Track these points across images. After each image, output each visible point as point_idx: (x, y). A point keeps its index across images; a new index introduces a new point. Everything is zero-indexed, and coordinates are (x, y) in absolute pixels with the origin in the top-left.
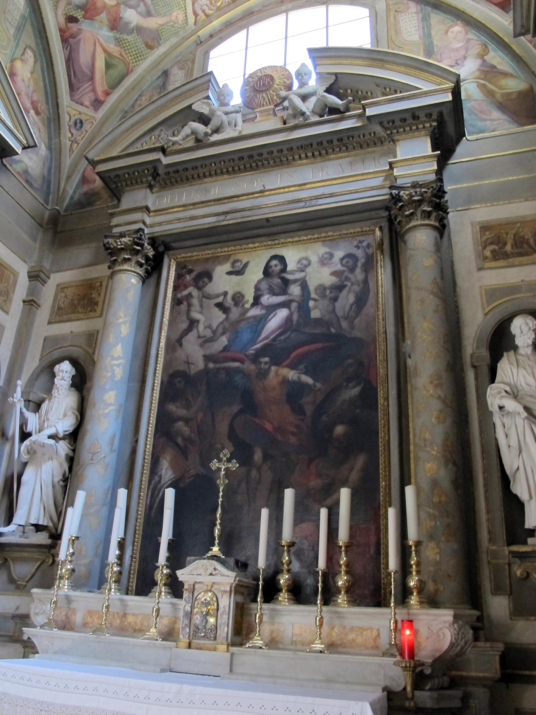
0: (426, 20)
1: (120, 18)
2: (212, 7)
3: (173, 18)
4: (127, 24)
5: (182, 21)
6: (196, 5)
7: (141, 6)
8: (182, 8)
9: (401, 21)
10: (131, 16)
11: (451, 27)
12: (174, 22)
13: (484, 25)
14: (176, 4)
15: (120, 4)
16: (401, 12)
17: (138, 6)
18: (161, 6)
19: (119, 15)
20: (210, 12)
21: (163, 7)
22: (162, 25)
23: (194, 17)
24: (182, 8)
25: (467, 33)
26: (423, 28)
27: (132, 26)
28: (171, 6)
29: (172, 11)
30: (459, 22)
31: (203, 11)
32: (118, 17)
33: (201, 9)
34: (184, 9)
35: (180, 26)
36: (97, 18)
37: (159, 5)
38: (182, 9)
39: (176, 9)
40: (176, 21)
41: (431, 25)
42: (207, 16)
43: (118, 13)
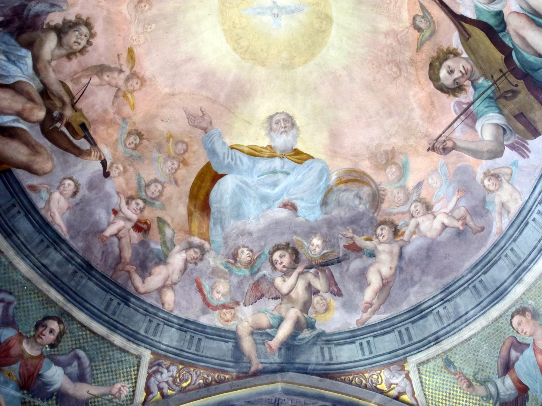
1: (39, 376)
2: (174, 387)
3: (115, 390)
4: (46, 385)
5: (126, 396)
6: (153, 379)
7: (73, 365)
8: (132, 379)
10: (55, 376)
12: (114, 395)
14: (123, 373)
15: (44, 357)
17: (70, 364)
18: (102, 371)
19: (39, 370)
20: (170, 392)
21: (104, 373)
22: (96, 397)
23: (145, 394)
24: (132, 379)
27: (52, 389)
28: (116, 375)
29: (115, 381)
31: (160, 389)
32: (36, 374)
33: (158, 385)
34: (134, 381)
35: (121, 403)
36: (6, 368)
37: (100, 369)
38: (130, 382)
39: (123, 379)
40: (117, 395)
42: (163, 396)
43: (37, 367)
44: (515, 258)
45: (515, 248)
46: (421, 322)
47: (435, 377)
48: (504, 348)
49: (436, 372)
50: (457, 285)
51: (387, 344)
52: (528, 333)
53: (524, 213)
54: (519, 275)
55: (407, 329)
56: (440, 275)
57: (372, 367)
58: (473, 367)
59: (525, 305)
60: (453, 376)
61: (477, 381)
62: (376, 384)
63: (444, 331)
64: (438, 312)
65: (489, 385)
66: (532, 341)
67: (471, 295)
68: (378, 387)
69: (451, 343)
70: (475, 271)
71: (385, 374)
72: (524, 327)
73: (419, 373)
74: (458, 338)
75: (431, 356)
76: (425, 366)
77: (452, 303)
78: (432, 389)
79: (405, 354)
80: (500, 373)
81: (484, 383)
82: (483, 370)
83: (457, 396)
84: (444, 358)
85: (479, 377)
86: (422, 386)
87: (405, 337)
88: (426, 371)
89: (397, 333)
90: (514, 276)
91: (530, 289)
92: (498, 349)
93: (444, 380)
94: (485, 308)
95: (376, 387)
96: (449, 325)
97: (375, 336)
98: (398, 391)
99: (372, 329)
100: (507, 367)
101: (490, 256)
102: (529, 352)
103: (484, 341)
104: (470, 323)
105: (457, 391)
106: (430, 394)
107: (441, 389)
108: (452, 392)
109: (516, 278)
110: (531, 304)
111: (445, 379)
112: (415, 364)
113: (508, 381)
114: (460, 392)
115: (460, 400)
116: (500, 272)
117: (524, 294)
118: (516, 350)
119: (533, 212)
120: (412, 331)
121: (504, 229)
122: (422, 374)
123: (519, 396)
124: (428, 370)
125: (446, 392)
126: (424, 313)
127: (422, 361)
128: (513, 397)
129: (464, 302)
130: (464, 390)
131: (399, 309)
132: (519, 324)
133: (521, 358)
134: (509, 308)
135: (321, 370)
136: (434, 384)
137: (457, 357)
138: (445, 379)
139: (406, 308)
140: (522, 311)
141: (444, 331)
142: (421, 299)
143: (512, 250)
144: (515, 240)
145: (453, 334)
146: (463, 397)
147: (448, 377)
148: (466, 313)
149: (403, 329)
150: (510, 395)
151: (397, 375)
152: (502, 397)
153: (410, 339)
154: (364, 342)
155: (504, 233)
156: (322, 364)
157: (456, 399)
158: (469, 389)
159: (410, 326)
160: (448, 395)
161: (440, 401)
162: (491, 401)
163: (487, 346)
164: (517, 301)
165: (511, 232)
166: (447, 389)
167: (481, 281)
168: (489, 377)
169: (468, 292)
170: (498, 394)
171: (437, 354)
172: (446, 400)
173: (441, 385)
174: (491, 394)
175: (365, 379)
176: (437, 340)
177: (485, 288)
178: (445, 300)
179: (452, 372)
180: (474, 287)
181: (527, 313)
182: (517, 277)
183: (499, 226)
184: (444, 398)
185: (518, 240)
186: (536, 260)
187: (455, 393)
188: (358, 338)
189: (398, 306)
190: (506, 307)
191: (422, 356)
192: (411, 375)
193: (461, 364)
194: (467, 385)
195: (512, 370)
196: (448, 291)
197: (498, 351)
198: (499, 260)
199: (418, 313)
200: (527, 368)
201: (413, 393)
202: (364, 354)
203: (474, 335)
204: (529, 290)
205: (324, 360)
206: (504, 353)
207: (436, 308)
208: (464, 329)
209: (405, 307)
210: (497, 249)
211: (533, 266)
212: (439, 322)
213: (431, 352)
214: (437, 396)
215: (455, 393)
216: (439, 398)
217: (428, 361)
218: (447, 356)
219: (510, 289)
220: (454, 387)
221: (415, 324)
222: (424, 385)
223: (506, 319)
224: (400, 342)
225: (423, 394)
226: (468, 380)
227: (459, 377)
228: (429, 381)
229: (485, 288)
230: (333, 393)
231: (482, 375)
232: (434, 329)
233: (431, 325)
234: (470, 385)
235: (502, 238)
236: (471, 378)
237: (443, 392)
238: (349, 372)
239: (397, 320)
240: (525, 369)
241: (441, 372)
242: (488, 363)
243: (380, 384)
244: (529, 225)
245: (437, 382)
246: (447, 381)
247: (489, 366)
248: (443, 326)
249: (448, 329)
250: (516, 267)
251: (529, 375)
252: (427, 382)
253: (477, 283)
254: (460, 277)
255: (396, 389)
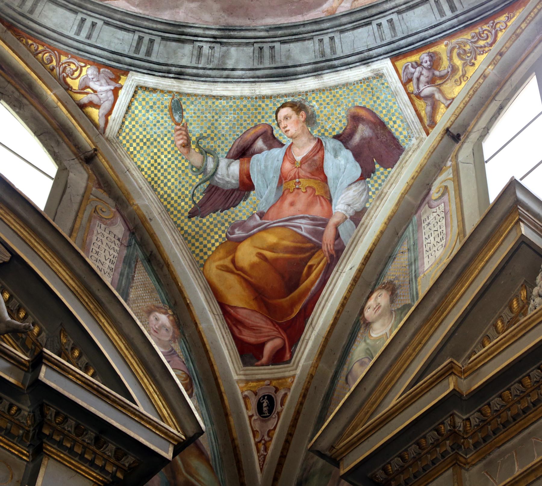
0: (130, 266)
9: (95, 232)
11: (158, 309)
13: (207, 351)
16: (101, 219)
25: (174, 339)
26: (122, 274)
30: (170, 312)
41: (133, 280)
44: (329, 50)
45: (337, 40)
46: (174, 44)
47: (151, 113)
48: (252, 132)
49: (155, 107)
50: (243, 34)
51: (116, 41)
52: (290, 133)
53: (374, 11)
54: (322, 69)
55: (152, 41)
56: (230, 10)
57: (78, 54)
58: (205, 129)
59: (306, 104)
60: (173, 124)
61: (198, 146)
62: (68, 76)
63: (195, 71)
64: (201, 48)
65: (210, 159)
66: (289, 144)
67: (251, 54)
68: (69, 80)
69: (194, 88)
70: (272, 33)
71: (89, 71)
72: (290, 125)
73: (133, 96)
74: (206, 89)
75: (160, 87)
76: (147, 93)
77: (224, 48)
78: (137, 122)
79: (130, 65)
80: (231, 155)
81: (205, 153)
82: (212, 139)
83: (162, 147)
84: (175, 99)
85: (203, 143)
86: (127, 112)
87: (143, 49)
88: (144, 99)
89: (136, 37)
90: (314, 66)
91: (324, 90)
92: (245, 128)
93: (158, 122)
94: (258, 77)
95: (64, 78)
96: (204, 69)
97: (106, 23)
98: (91, 99)
99: (109, 13)
100: (243, 152)
101: (302, 29)
102: (278, 153)
103: (234, 110)
104: (231, 82)
105: (166, 142)
106: (130, 126)
107: (148, 129)
108: (159, 139)
109: (315, 70)
110: (313, 107)
111: (162, 122)
112: (135, 84)
113: (235, 167)
114: (169, 146)
115: (162, 153)
116: (302, 53)
117: (313, 91)
118: (265, 142)
119: (384, 16)
120: (156, 47)
121: (337, 12)
122: (135, 99)
123: (238, 190)
124: (147, 99)
125: (152, 136)
126: (184, 37)
127: (146, 85)
128: (229, 187)
129: (238, 56)
130: (175, 146)
131: (158, 13)
132: (286, 118)
133: (265, 153)
134: (286, 95)
135: (8, 15)
136: (144, 118)
137: (192, 107)
138: (162, 122)
139: (166, 18)
140: (298, 107)
141: (195, 71)
142: (191, 21)
143: (332, 39)
144: (342, 31)
145: (203, 81)
146: (169, 153)
147: (166, 122)
148: (233, 70)
149: (147, 38)
150: (227, 182)
151: (103, 81)
152: (216, 179)
153: (149, 53)
154: (89, 21)
155: (334, 16)
156: (14, 10)
157: (159, 150)
158: (182, 149)
159: (158, 40)
160: (152, 140)
161: (138, 141)
162: (200, 176)
163: (234, 118)
164: (299, 94)
165: (344, 20)
166: (155, 133)
167: (272, 48)
168: (215, 150)
169: (249, 50)
170: (215, 173)
171: (169, 89)
172: (145, 144)
173: (152, 125)
174: (205, 169)
175: (59, 61)
176: (180, 75)
177: (272, 57)
178: (218, 40)
179: (174, 119)
180: (261, 49)
181: (303, 113)
182: (318, 69)
183: (335, 5)
184: (145, 140)
185: (346, 34)
186: (351, 66)
187: (162, 143)
188: (85, 11)
189: (158, 9)
190: (283, 92)
191: (150, 81)
192: (121, 93)
193: (191, 117)
194: (183, 143)
195: (246, 159)
196: (227, 33)
197: (244, 131)
198: (309, 39)
199: (178, 33)
200: (266, 167)
201: (110, 113)
202: (78, 34)
203: (226, 98)
204: (321, 90)
205: (20, 6)
206: (249, 137)
207: (201, 41)
208: (219, 84)
209: (166, 16)
210: (315, 27)
211: (343, 70)
212: (194, 59)
213: (165, 83)
214: (137, 134)
215: (162, 143)
216: (138, 137)
217: (154, 90)
218: (181, 99)
219: (300, 76)
220: (166, 135)
221: (164, 42)
222: (130, 113)
223: (274, 105)
224: (133, 49)
225: (121, 121)
226: (188, 139)
227: (180, 129)
228: (140, 111)
229: (272, 57)
230: (10, 52)
231: (208, 143)
232: (184, 62)
233: (184, 55)
234: (187, 145)
235: (330, 20)
236: (194, 139)
237: (148, 133)
238: (42, 41)
239: (146, 23)
240: (262, 167)
241: (162, 111)
242: (223, 135)
243: (72, 79)
244: (370, 27)
245: (148, 119)
246: (162, 125)
247: (223, 139)
248: (196, 65)
249: (201, 72)
250: (324, 59)
251: (263, 175)
252: (136, 112)
253: (266, 46)
254: (251, 27)
255: (89, 95)
